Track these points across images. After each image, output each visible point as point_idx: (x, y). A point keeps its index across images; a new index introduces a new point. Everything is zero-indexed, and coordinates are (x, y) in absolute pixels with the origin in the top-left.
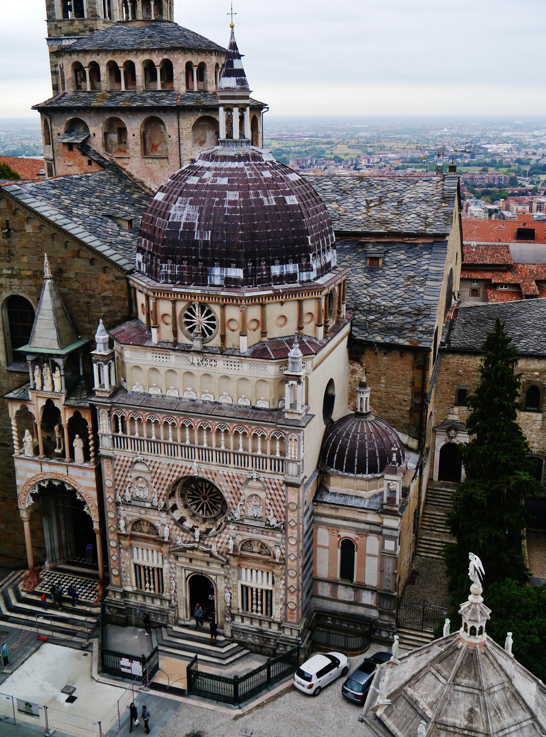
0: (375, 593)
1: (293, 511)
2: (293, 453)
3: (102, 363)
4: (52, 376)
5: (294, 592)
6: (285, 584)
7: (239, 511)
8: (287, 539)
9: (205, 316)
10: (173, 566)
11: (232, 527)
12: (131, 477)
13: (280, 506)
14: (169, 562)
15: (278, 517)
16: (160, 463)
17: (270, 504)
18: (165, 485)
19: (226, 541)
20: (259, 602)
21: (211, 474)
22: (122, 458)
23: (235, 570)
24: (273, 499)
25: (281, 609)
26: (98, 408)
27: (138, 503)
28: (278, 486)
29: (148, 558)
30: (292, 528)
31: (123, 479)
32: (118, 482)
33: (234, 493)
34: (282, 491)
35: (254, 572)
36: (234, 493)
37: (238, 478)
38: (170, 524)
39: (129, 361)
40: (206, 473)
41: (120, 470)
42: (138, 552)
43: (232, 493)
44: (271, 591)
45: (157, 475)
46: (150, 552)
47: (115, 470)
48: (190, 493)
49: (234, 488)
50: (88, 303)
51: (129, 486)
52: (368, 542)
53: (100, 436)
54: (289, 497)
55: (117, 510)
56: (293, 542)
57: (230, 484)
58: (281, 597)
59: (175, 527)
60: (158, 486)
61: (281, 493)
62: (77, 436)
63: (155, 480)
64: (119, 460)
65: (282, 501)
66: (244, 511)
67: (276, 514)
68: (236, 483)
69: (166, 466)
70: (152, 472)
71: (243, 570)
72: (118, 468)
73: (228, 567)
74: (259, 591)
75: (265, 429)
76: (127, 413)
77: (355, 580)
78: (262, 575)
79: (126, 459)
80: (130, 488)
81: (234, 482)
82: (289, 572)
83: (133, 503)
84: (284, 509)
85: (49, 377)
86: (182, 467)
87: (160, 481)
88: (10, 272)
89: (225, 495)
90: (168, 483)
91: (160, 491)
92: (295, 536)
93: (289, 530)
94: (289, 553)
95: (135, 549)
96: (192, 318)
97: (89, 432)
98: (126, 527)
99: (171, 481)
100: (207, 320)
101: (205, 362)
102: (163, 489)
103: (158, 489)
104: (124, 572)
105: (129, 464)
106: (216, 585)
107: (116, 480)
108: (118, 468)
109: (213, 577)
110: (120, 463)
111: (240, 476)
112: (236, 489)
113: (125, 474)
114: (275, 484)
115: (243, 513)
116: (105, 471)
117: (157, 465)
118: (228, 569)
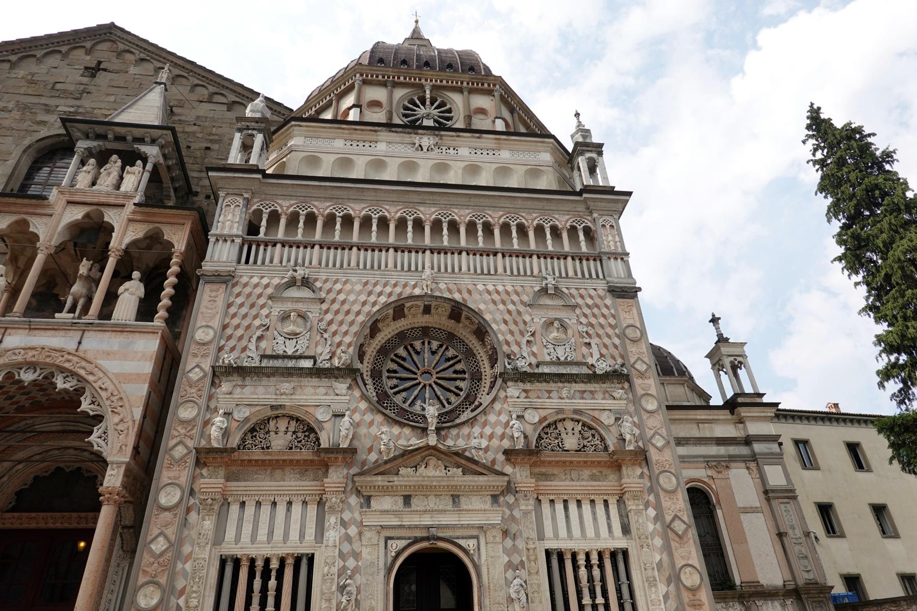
0: (789, 602)
1: (634, 341)
2: (612, 243)
3: (255, 132)
4: (123, 169)
5: (686, 531)
6: (659, 518)
7: (525, 354)
8: (636, 401)
9: (436, 108)
10: (353, 531)
11: (513, 390)
12: (267, 316)
13: (609, 336)
14: (344, 524)
15: (608, 356)
16: (346, 282)
17: (587, 332)
18: (352, 323)
19: (499, 431)
20: (600, 600)
21: (460, 291)
22: (255, 280)
23: (527, 505)
24: (592, 325)
25: (666, 597)
26: (222, 194)
27: (278, 363)
28: (598, 301)
29: (271, 533)
30: (642, 375)
31: (246, 323)
32: (229, 331)
33: (511, 323)
34: (607, 307)
35: (573, 507)
36: (511, 323)
37: (517, 293)
38: (354, 411)
39: (301, 148)
40: (450, 291)
41: (242, 305)
42: (241, 520)
43: (505, 322)
44: (625, 553)
45: (336, 306)
46: (281, 509)
47: (229, 306)
48: (394, 366)
49: (509, 312)
50: (208, 148)
51: (259, 333)
52: (733, 482)
53: (212, 240)
54: (622, 318)
55: (210, 397)
56: (652, 405)
57: (501, 307)
58: (657, 558)
59: (368, 417)
60: (333, 328)
61: (605, 311)
62: (136, 274)
63: (329, 317)
64: (245, 285)
65: (610, 325)
66: (534, 355)
67: (604, 351)
68: (513, 303)
69: (358, 287)
70: (322, 301)
71: (546, 508)
72: (239, 301)
73: (510, 499)
74: (595, 560)
75: (557, 216)
76: (286, 203)
77: (738, 582)
78: (594, 514)
79: (265, 281)
80: (260, 338)
81: (508, 302)
82: (661, 481)
83: (265, 363)
84: (617, 341)
85: (115, 174)
86: (395, 285)
87: (340, 317)
88: (72, 110)
89: (494, 326)
90: (361, 318)
91: (337, 339)
92: (653, 391)
93: (637, 382)
94: (649, 433)
95: (235, 509)
96: (415, 111)
97: (174, 260)
98: (226, 433)
99: (368, 313)
100: (439, 112)
101: (436, 150)
102: (346, 333)
103: (335, 333)
104: (182, 592)
105: (270, 291)
106: (477, 568)
107: (225, 327)
108: (239, 301)
109: (470, 544)
110: (248, 290)
111: (519, 289)
112: (515, 314)
113: (254, 312)
114: (591, 297)
115: (534, 361)
116: (203, 309)
117: (338, 286)
118: (510, 507)
